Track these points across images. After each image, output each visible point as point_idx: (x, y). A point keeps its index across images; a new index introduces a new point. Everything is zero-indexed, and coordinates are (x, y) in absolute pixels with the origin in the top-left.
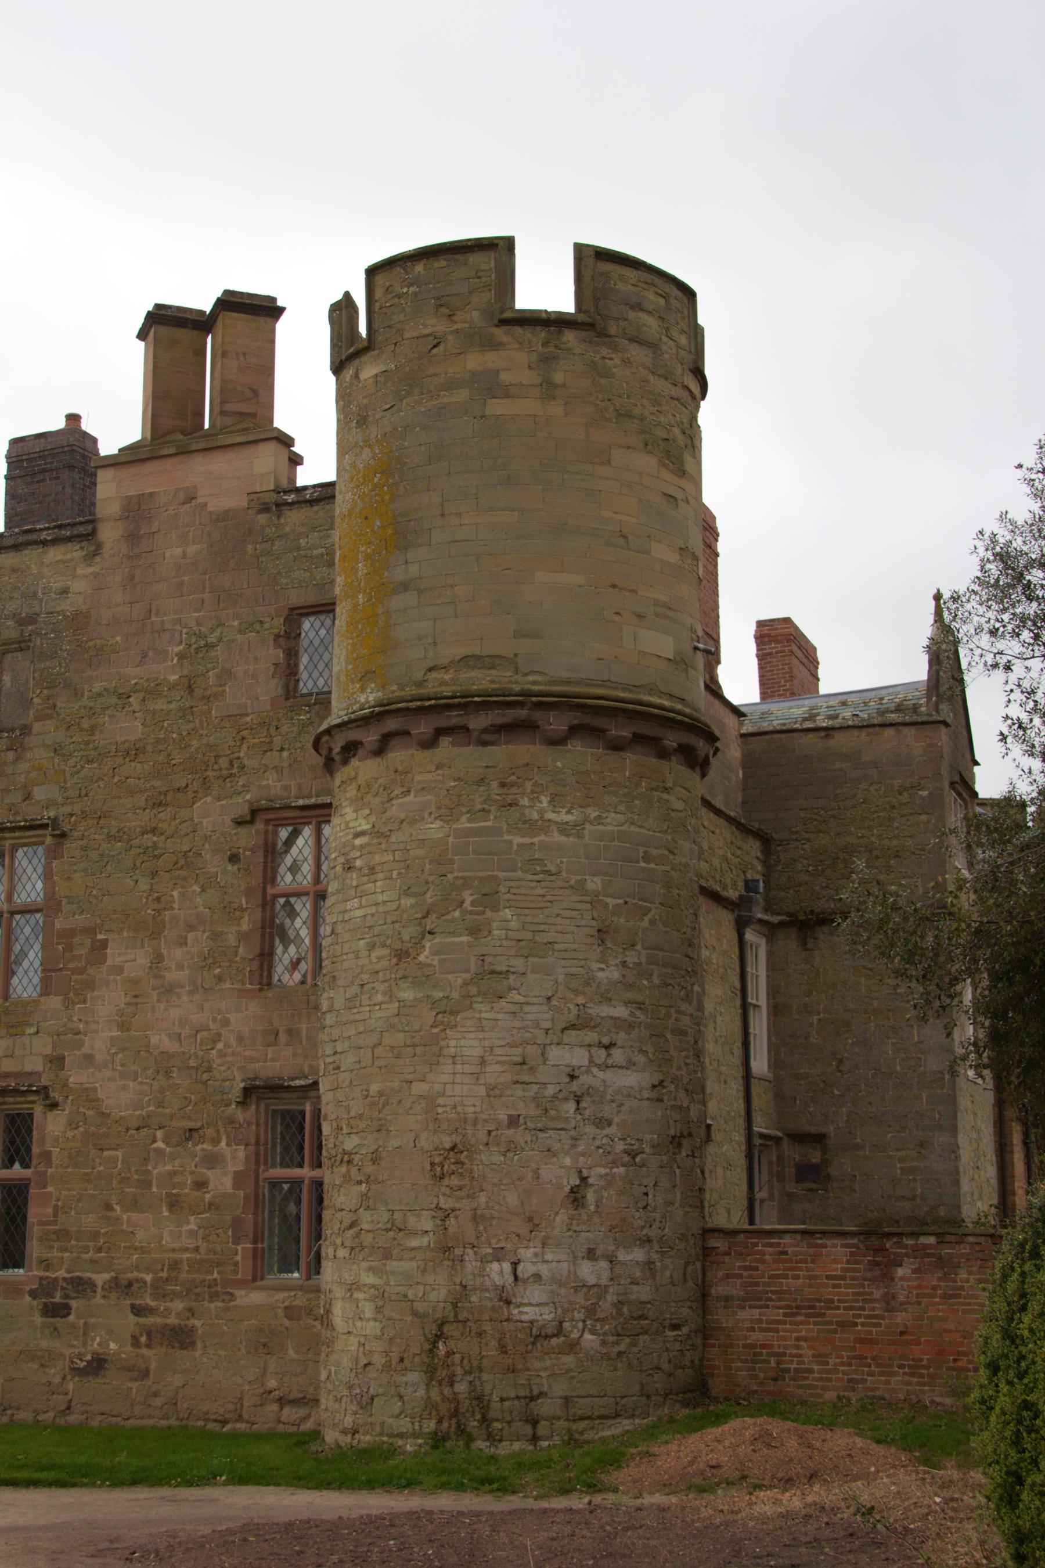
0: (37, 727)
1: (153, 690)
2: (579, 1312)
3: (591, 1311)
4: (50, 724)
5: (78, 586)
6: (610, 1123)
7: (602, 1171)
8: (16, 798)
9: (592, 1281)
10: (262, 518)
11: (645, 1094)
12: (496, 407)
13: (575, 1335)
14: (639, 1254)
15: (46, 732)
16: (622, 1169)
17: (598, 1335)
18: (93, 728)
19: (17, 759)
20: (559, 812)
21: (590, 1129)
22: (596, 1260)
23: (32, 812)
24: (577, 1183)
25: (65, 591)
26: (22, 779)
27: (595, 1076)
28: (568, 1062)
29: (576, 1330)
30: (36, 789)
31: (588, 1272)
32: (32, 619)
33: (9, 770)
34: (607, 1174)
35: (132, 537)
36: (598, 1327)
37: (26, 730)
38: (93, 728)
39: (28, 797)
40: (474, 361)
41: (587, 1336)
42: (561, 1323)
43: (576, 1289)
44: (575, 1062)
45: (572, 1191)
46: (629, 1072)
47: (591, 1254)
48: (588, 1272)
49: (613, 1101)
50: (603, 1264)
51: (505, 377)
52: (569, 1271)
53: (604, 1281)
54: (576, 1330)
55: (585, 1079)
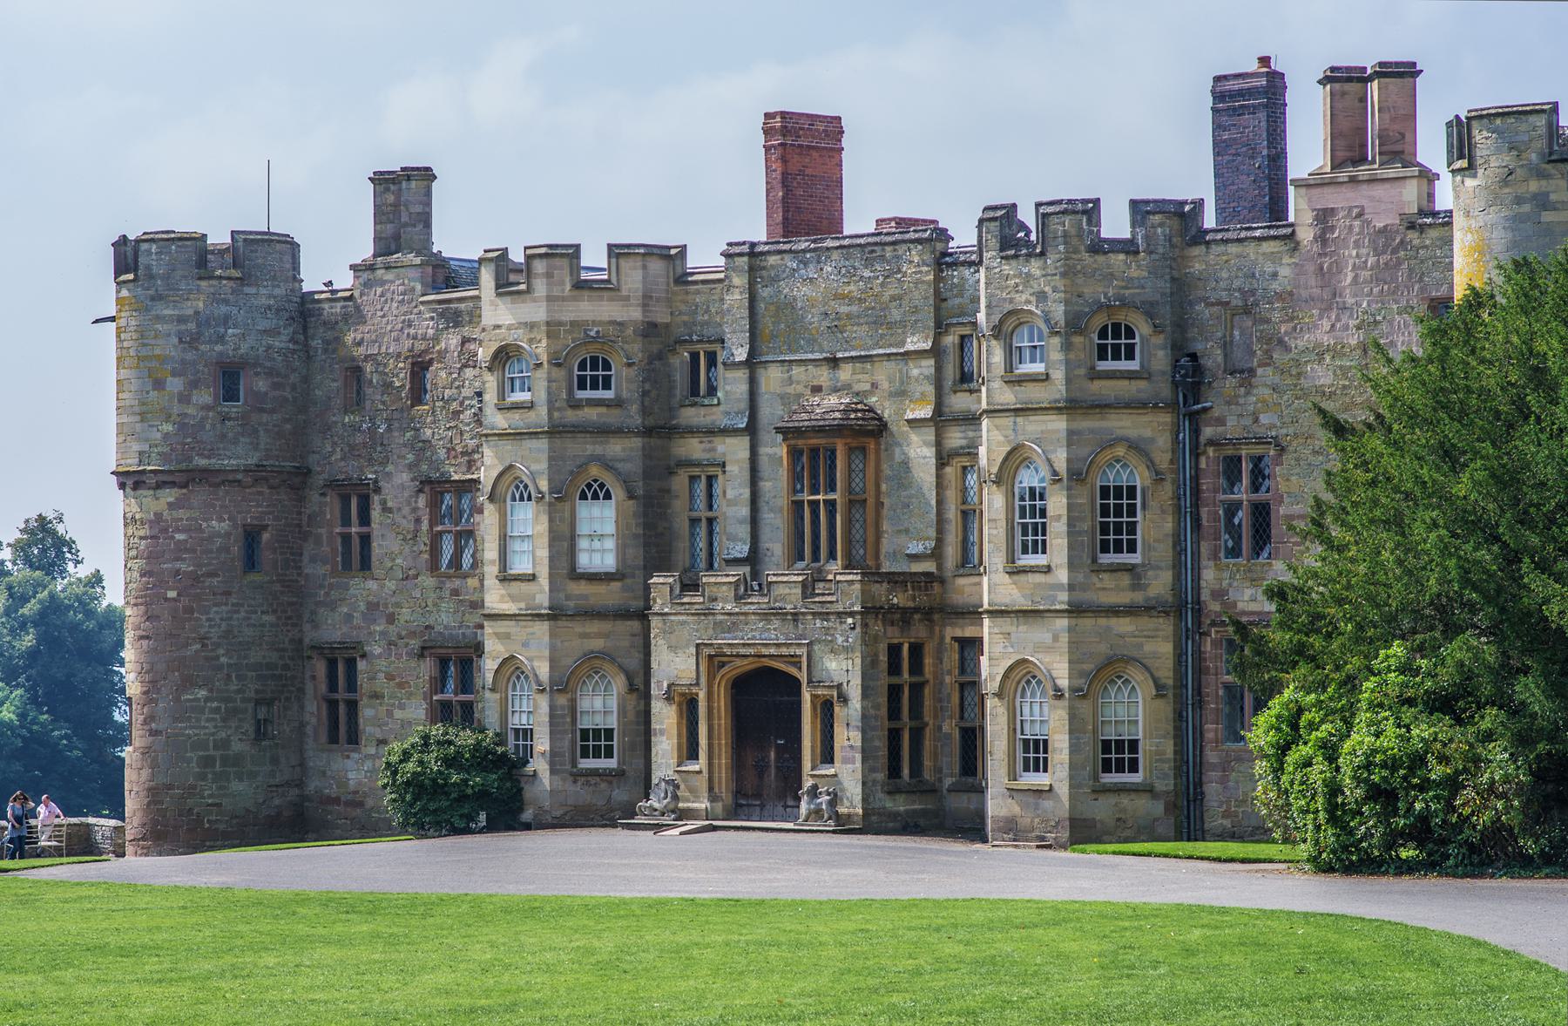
0: (1260, 371)
1: (1337, 351)
4: (1269, 370)
5: (1284, 271)
8: (1248, 421)
10: (1412, 236)
12: (1547, 217)
15: (1265, 375)
18: (1299, 374)
19: (1248, 393)
23: (1261, 431)
25: (1275, 275)
26: (1251, 408)
30: (1261, 416)
32: (1253, 292)
33: (1241, 401)
35: (1322, 239)
37: (1252, 372)
38: (1299, 374)
39: (1256, 420)
40: (1534, 186)
51: (1553, 197)
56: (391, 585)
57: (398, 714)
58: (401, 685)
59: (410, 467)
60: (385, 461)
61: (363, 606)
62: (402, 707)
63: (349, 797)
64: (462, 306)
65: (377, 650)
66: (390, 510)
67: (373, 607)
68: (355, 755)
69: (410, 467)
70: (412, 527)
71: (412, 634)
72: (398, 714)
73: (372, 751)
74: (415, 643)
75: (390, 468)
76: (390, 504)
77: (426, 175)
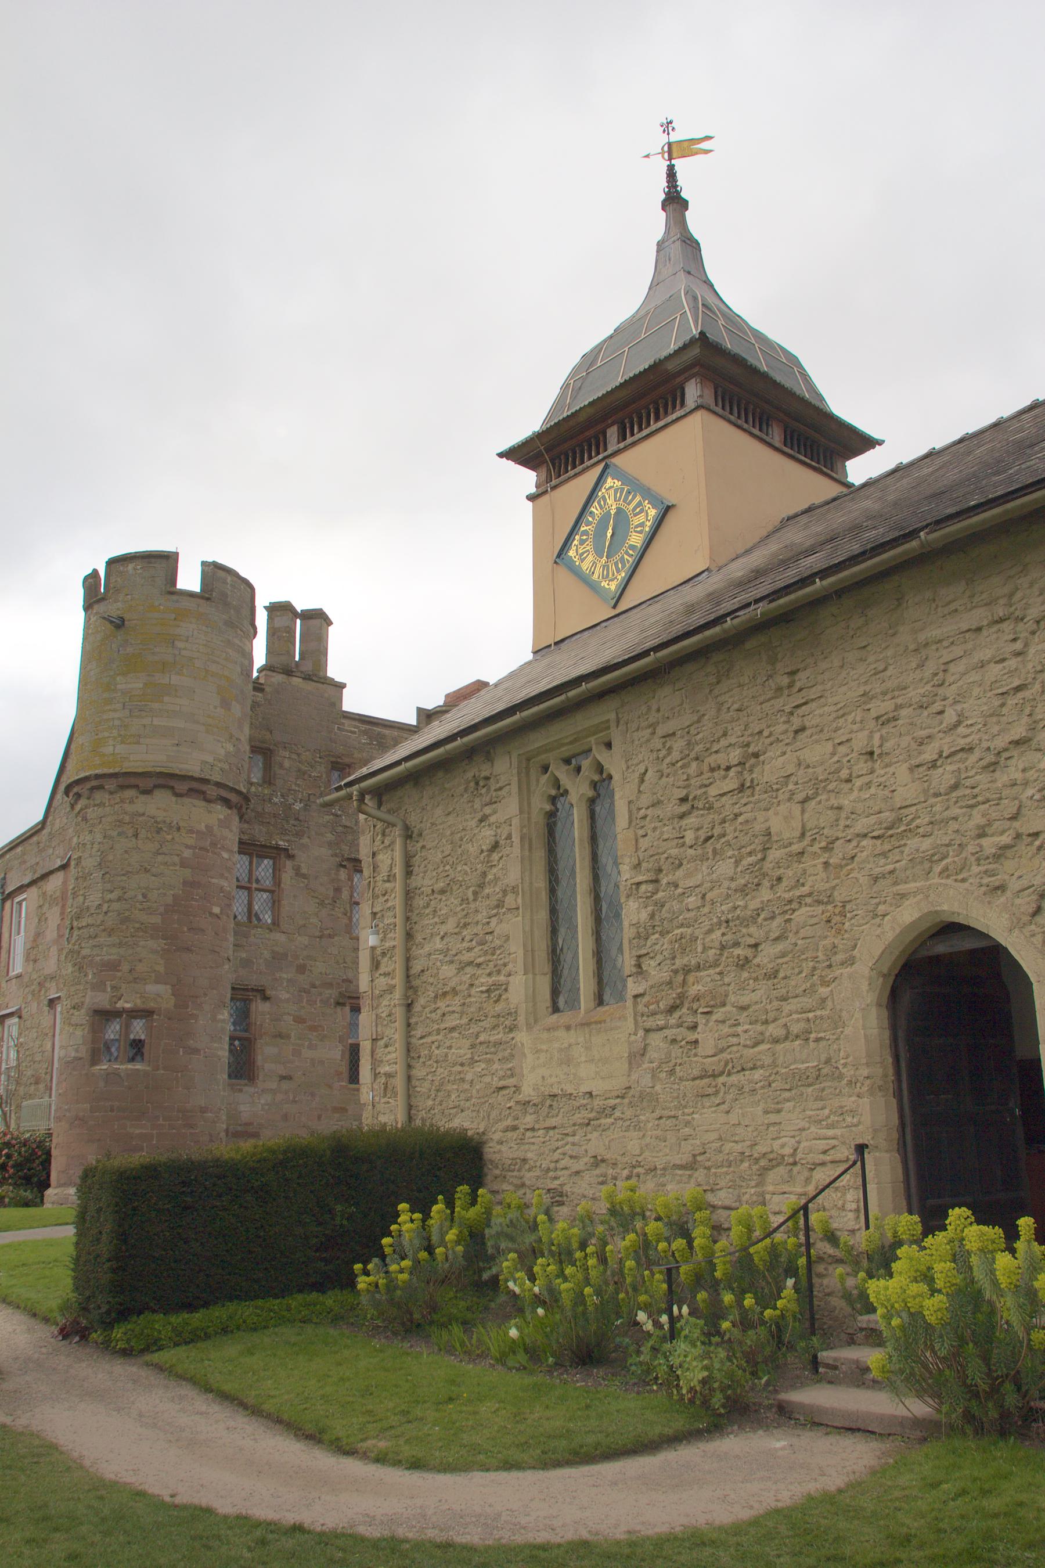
56: (304, 940)
57: (307, 1053)
58: (314, 1028)
59: (330, 844)
60: (299, 834)
61: (267, 954)
62: (311, 1047)
63: (239, 1128)
64: (387, 732)
65: (284, 995)
66: (304, 876)
67: (278, 958)
68: (251, 1090)
69: (330, 844)
70: (331, 893)
71: (330, 985)
72: (307, 1053)
73: (274, 1085)
74: (332, 993)
75: (305, 840)
76: (304, 871)
77: (317, 619)
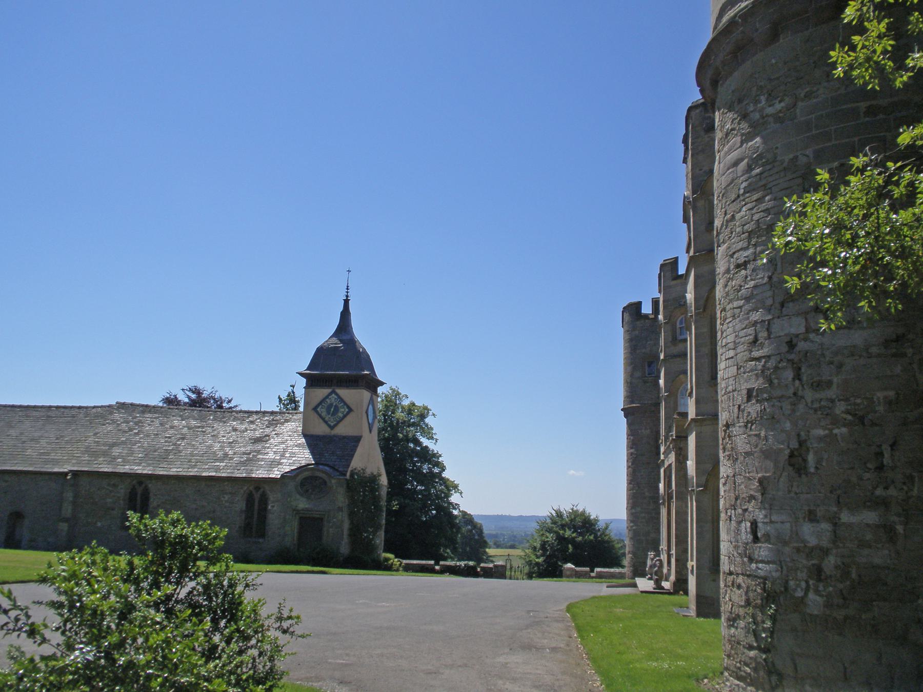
2: (802, 572)
3: (818, 573)
6: (829, 384)
7: (821, 432)
9: (813, 541)
11: (874, 350)
13: (799, 593)
14: (870, 517)
16: (844, 430)
17: (821, 596)
20: (773, 105)
21: (809, 395)
22: (818, 522)
24: (797, 447)
27: (812, 342)
28: (786, 332)
29: (799, 589)
31: (811, 534)
34: (826, 436)
36: (821, 588)
41: (811, 595)
42: (787, 582)
43: (798, 550)
44: (793, 331)
45: (791, 455)
46: (852, 331)
47: (812, 517)
48: (811, 534)
49: (832, 363)
50: (825, 526)
52: (791, 531)
53: (825, 543)
54: (799, 589)
55: (802, 345)
